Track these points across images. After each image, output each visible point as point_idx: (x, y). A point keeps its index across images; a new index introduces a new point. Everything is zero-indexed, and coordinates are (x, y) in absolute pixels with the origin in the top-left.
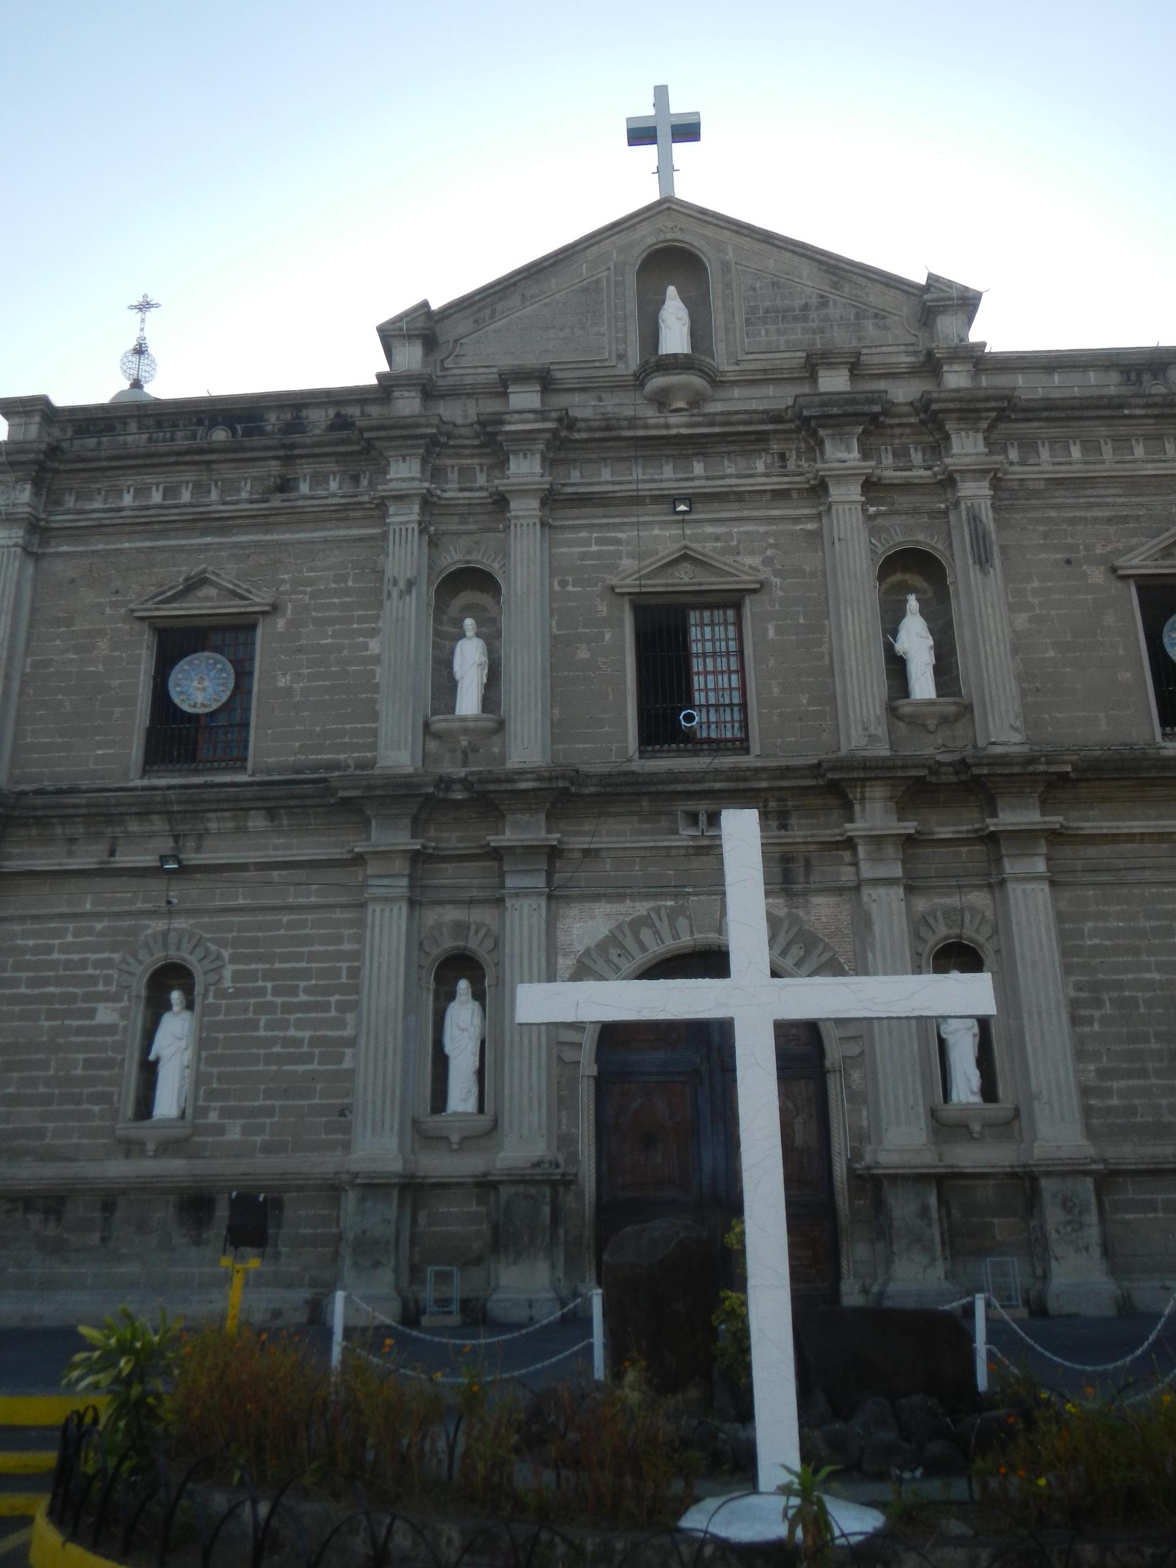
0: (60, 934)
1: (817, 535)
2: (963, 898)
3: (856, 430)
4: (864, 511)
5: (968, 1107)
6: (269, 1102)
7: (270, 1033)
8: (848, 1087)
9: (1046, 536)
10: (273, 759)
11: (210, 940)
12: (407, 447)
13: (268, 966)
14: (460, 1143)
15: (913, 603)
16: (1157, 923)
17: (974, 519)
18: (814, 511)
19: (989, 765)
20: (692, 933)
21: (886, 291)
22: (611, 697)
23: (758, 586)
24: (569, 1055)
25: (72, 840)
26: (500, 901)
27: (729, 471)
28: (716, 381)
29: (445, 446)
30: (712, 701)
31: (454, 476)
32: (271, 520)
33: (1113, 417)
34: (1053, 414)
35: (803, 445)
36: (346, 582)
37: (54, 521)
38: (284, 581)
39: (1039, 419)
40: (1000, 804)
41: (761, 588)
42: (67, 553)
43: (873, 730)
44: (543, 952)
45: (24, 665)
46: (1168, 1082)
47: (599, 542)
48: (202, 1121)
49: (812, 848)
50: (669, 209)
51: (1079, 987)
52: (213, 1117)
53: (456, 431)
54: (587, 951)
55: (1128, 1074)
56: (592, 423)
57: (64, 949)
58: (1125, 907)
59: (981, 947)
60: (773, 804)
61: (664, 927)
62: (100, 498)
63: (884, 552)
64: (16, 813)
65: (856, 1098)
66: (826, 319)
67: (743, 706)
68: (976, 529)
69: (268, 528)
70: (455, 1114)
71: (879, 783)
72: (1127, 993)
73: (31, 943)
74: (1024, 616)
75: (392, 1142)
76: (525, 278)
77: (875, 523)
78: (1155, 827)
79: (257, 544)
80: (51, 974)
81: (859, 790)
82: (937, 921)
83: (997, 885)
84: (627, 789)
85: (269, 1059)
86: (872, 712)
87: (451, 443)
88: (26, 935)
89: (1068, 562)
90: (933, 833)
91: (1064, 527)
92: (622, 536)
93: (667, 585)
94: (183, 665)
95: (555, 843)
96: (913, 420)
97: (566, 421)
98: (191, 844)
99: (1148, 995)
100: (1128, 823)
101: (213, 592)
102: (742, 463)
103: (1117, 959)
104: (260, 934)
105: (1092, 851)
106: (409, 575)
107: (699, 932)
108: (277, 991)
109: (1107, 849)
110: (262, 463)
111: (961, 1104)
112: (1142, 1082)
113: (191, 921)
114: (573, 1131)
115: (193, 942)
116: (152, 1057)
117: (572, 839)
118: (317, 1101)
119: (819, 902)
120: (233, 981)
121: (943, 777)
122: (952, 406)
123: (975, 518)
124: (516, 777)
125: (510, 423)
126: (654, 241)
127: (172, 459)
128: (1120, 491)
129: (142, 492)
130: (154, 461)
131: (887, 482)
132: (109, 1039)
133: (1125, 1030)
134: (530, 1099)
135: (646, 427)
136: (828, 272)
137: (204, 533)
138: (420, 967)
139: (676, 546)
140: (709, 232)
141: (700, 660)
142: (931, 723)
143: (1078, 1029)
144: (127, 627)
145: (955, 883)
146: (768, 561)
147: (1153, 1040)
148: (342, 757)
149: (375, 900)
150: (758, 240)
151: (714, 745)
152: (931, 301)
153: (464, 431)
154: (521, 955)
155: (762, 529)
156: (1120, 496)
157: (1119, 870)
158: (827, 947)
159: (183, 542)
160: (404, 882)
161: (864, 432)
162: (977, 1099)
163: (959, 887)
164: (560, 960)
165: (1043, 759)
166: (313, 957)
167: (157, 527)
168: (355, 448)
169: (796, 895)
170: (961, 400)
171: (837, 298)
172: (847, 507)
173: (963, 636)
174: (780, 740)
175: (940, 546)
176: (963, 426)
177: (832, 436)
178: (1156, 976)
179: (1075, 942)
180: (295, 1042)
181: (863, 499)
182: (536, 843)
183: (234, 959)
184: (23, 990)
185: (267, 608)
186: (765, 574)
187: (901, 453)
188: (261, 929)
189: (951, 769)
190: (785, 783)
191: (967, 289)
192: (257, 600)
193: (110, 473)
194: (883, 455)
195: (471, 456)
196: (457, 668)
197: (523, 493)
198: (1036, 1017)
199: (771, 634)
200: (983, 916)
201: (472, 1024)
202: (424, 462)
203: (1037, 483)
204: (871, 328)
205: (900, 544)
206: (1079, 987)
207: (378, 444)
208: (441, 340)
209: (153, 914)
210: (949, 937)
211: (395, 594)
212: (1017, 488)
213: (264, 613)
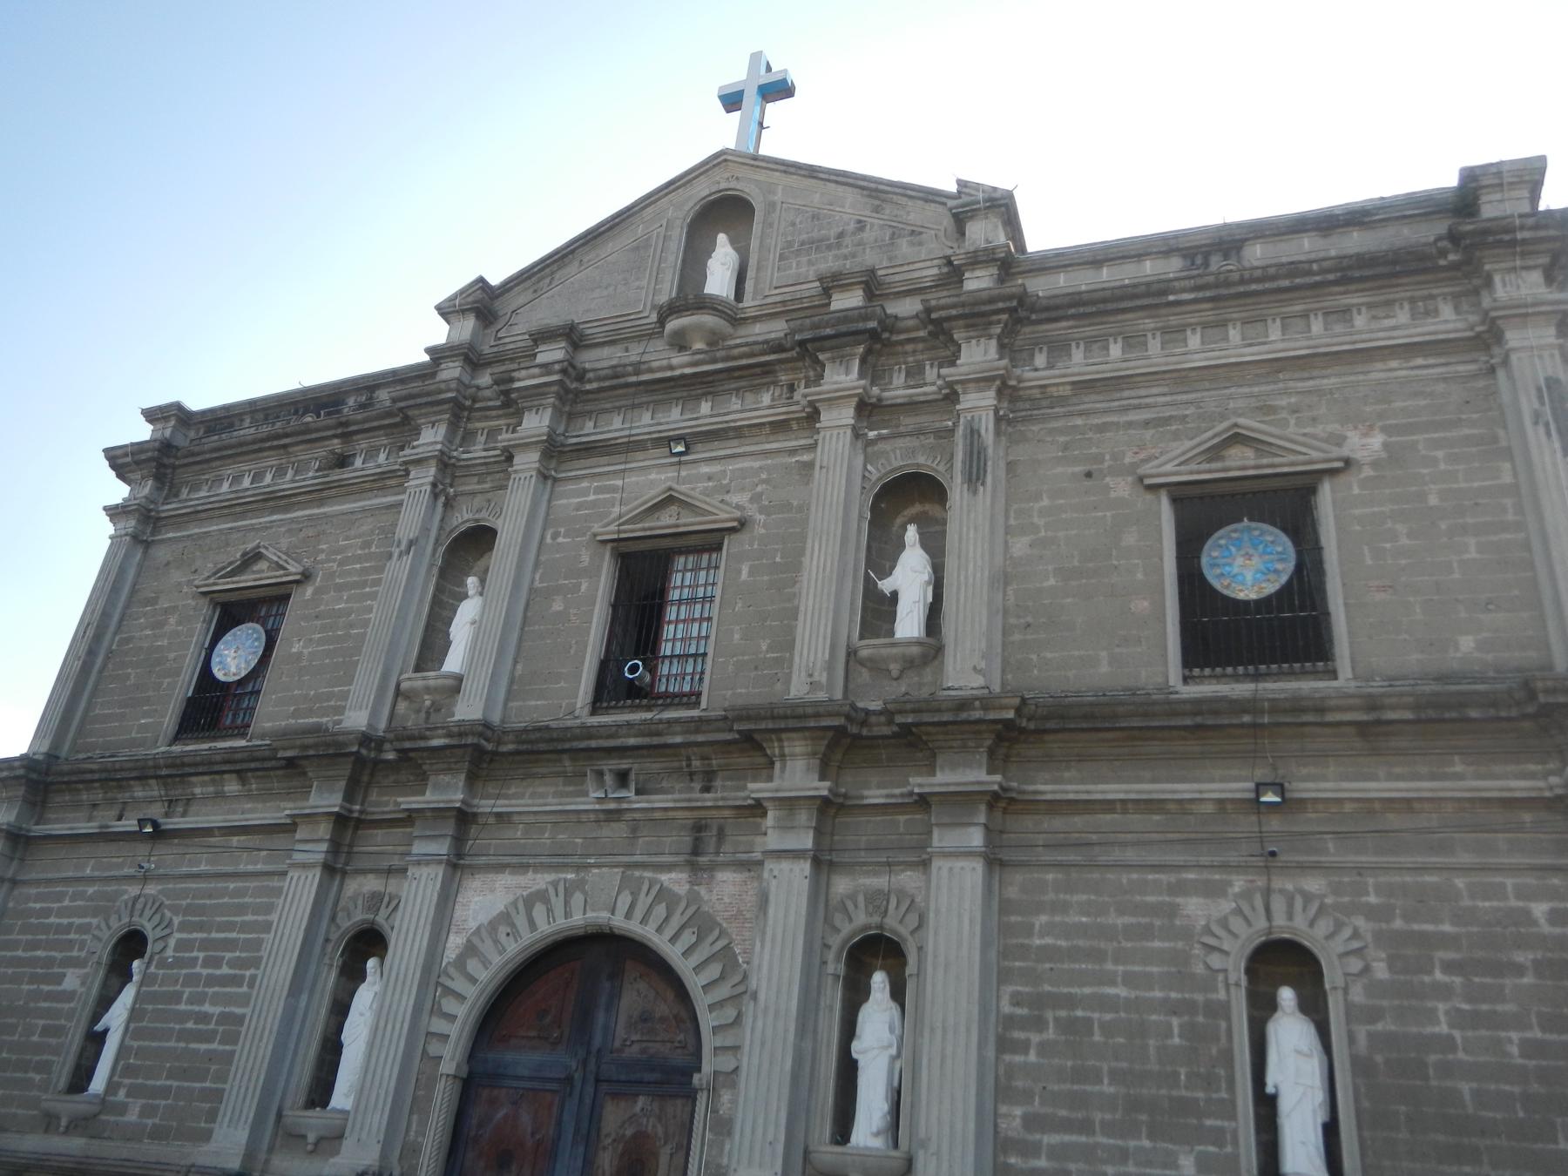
0: (60, 897)
1: (810, 465)
2: (893, 879)
4: (857, 435)
5: (865, 1154)
6: (169, 1083)
7: (190, 1007)
8: (715, 1111)
9: (1066, 447)
10: (270, 724)
11: (170, 908)
12: (435, 413)
13: (205, 935)
14: (316, 1144)
15: (912, 533)
16: (1133, 920)
17: (973, 433)
18: (810, 441)
19: (913, 711)
21: (927, 206)
22: (572, 652)
23: (735, 524)
24: (434, 1049)
25: (95, 805)
26: (404, 871)
27: (736, 407)
28: (736, 320)
29: (471, 409)
30: (677, 652)
31: (481, 439)
32: (325, 494)
33: (1157, 306)
34: (1081, 310)
35: (811, 373)
36: (370, 548)
37: (164, 511)
38: (322, 551)
39: (1067, 318)
40: (939, 761)
41: (742, 525)
42: (170, 539)
43: (816, 677)
44: (428, 927)
45: (111, 645)
46: (1120, 1142)
47: (598, 490)
48: (112, 1098)
49: (727, 813)
50: (726, 160)
51: (1017, 1001)
52: (121, 1095)
53: (480, 394)
55: (1067, 1126)
56: (600, 372)
57: (61, 913)
58: (1093, 897)
59: (905, 940)
60: (696, 763)
61: (558, 904)
62: (206, 488)
63: (880, 479)
64: (49, 779)
65: (723, 1127)
66: (860, 244)
67: (705, 654)
68: (972, 444)
69: (321, 502)
70: (335, 1110)
71: (794, 735)
72: (1079, 1013)
73: (38, 906)
74: (1026, 540)
75: (242, 1135)
76: (583, 245)
77: (876, 448)
78: (1138, 792)
79: (310, 518)
80: (44, 937)
82: (856, 907)
83: (925, 864)
84: (542, 746)
85: (184, 1035)
86: (820, 655)
87: (477, 406)
88: (39, 898)
89: (1089, 475)
90: (863, 797)
91: (1090, 435)
92: (619, 483)
93: (644, 529)
94: (228, 637)
95: (458, 805)
96: (922, 333)
97: (570, 369)
98: (180, 809)
99: (1108, 1017)
100: (1101, 787)
101: (263, 565)
102: (749, 397)
103: (1072, 966)
104: (208, 902)
105: (1058, 823)
106: (411, 536)
107: (593, 910)
108: (208, 963)
109: (1078, 821)
110: (327, 443)
111: (857, 1148)
112: (1083, 1139)
113: (160, 887)
114: (420, 1139)
115: (157, 904)
116: (99, 1027)
117: (483, 802)
118: (208, 1084)
120: (175, 950)
121: (875, 729)
122: (954, 312)
123: (972, 431)
124: (428, 733)
125: (519, 380)
126: (707, 192)
127: (256, 447)
128: (1166, 390)
129: (237, 479)
130: (245, 449)
131: (889, 402)
132: (66, 1006)
133: (1069, 1063)
134: (378, 1095)
135: (651, 370)
136: (869, 196)
137: (274, 510)
138: (327, 940)
139: (663, 487)
140: (762, 176)
141: (674, 608)
142: (895, 668)
143: (1007, 1057)
144: (193, 603)
146: (756, 498)
147: (1106, 1081)
148: (325, 720)
149: (294, 866)
150: (804, 176)
151: (669, 700)
152: (956, 208)
153: (487, 393)
154: (408, 930)
155: (757, 464)
156: (1164, 395)
157: (1089, 844)
158: (722, 933)
159: (254, 521)
160: (324, 847)
161: (869, 352)
162: (878, 1143)
163: (889, 864)
164: (452, 937)
165: (977, 703)
166: (245, 927)
167: (238, 509)
168: (398, 419)
170: (963, 305)
171: (876, 221)
172: (835, 432)
173: (951, 563)
174: (730, 692)
175: (941, 468)
176: (972, 334)
177: (833, 360)
178: (1122, 991)
179: (1021, 941)
180: (204, 1018)
181: (852, 422)
182: (442, 805)
183: (184, 927)
184: (20, 953)
185: (297, 577)
186: (752, 511)
187: (915, 372)
188: (210, 897)
189: (883, 719)
190: (700, 738)
191: (995, 189)
192: (292, 569)
193: (214, 464)
194: (895, 375)
195: (498, 417)
196: (453, 629)
197: (526, 446)
198: (939, 1033)
199: (744, 575)
200: (913, 901)
201: (371, 1007)
202: (453, 426)
203: (1061, 388)
204: (905, 245)
205: (901, 467)
206: (1017, 1001)
207: (410, 413)
208: (501, 313)
209: (129, 879)
210: (867, 927)
211: (396, 555)
213: (297, 582)
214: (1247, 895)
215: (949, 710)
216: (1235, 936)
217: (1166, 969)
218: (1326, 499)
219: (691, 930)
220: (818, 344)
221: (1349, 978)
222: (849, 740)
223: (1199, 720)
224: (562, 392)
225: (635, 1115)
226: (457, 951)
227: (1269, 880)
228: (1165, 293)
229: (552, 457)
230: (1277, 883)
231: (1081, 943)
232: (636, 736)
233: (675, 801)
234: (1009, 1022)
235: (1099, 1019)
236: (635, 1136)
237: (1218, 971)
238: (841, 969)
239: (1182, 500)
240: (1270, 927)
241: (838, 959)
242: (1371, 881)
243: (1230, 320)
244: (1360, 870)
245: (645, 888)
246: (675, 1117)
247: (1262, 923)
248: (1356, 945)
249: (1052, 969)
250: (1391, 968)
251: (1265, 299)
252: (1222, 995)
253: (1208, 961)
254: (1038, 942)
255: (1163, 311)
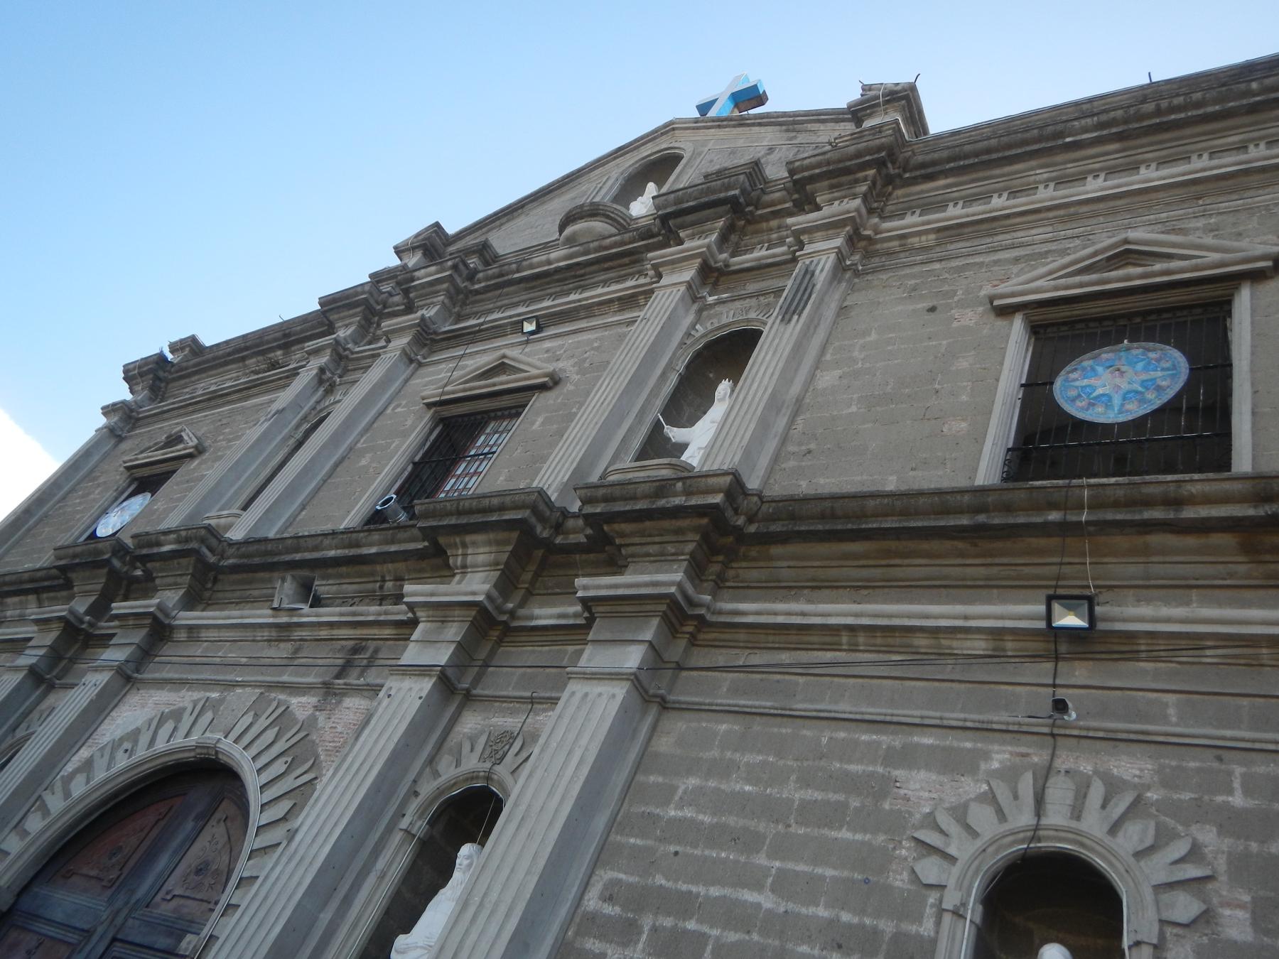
3: (717, 225)
16: (818, 795)
17: (809, 273)
19: (607, 499)
50: (674, 129)
63: (703, 336)
72: (691, 925)
81: (460, 552)
82: (472, 750)
89: (932, 309)
90: (532, 618)
96: (787, 205)
97: (461, 266)
99: (733, 937)
103: (707, 852)
121: (571, 536)
124: (162, 538)
125: (419, 279)
136: (787, 131)
145: (528, 694)
150: (734, 126)
163: (532, 701)
167: (191, 409)
176: (836, 194)
178: (767, 901)
179: (651, 809)
190: (393, 548)
203: (924, 238)
210: (473, 776)
212: (898, 249)
214: (1010, 775)
215: (645, 497)
216: (974, 834)
217: (846, 874)
218: (1244, 300)
220: (679, 220)
221: (1169, 931)
222: (539, 553)
223: (981, 518)
224: (452, 290)
227: (1053, 756)
228: (1060, 135)
229: (425, 345)
230: (1065, 761)
231: (732, 820)
232: (337, 548)
233: (342, 615)
234: (592, 923)
235: (718, 938)
237: (930, 886)
238: (420, 827)
239: (1046, 326)
240: (1037, 828)
241: (421, 813)
242: (1238, 770)
243: (1143, 162)
244: (1220, 750)
247: (1025, 818)
248: (1192, 871)
249: (676, 853)
250: (1257, 922)
251: (1188, 131)
252: (927, 928)
253: (917, 869)
254: (672, 813)
255: (1059, 158)
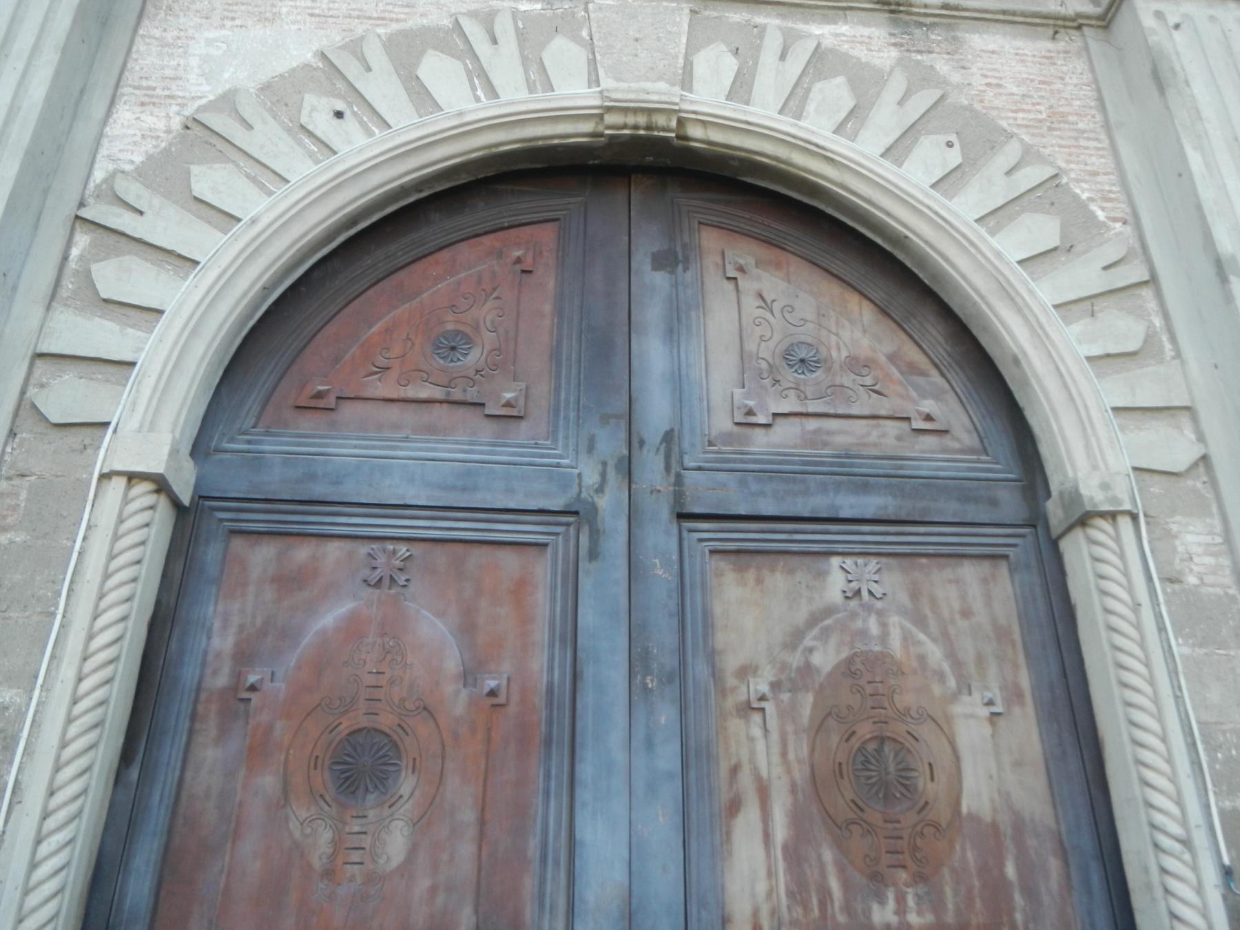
20: (594, 80)
44: (49, 61)
54: (227, 102)
119: (991, 47)
164: (124, 115)
169: (921, 25)
219: (943, 138)
225: (829, 611)
226: (149, 146)
236: (849, 669)
245: (773, 43)
246: (966, 613)
